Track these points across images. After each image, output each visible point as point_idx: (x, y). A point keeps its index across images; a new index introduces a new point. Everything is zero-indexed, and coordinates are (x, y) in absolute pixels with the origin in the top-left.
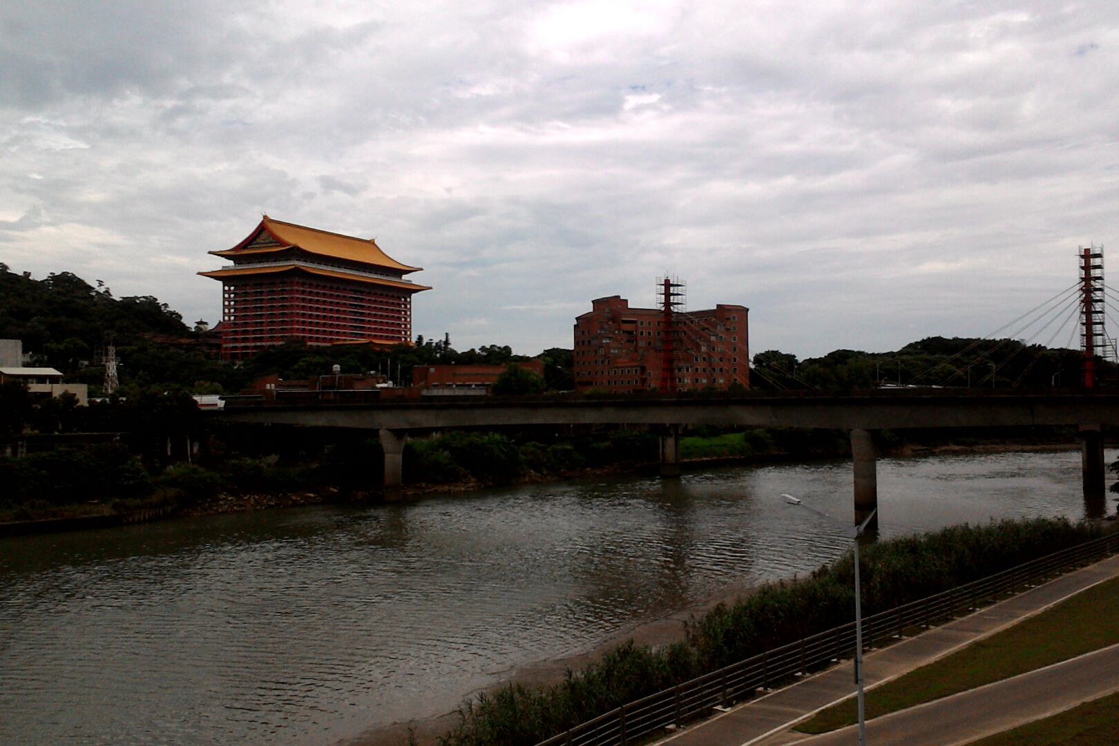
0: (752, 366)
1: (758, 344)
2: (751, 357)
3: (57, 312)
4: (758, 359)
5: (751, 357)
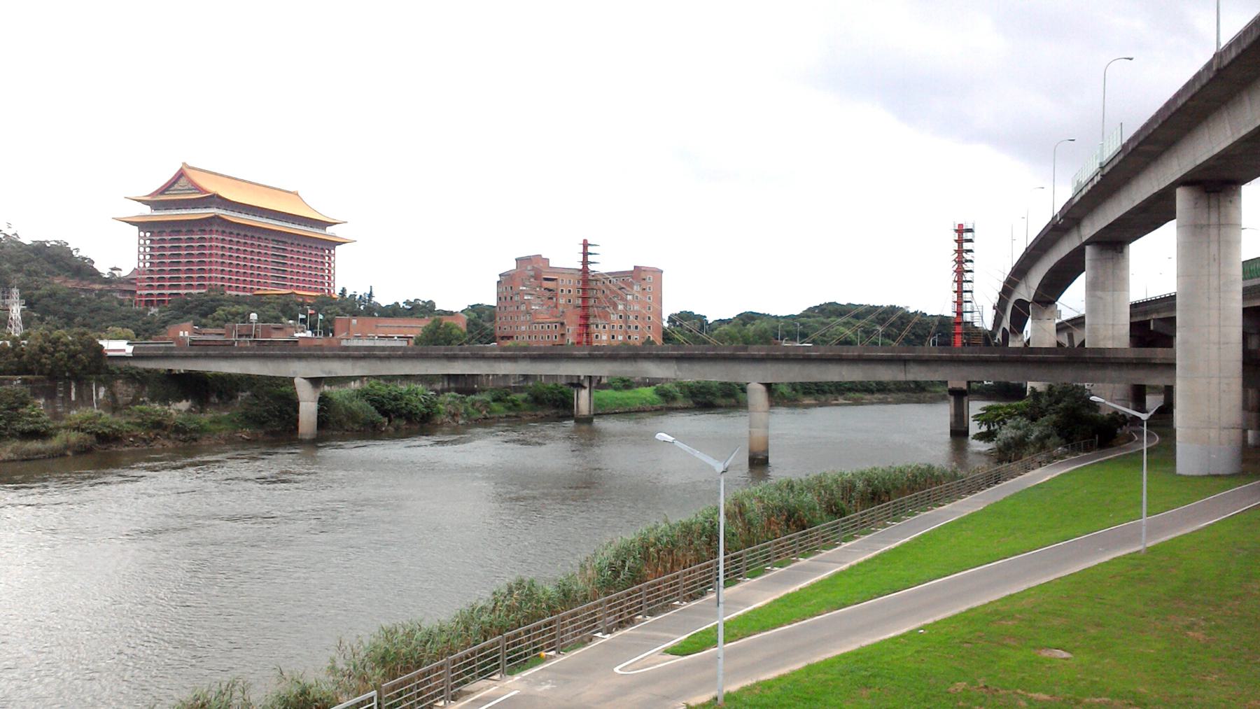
0: (666, 324)
1: (670, 307)
2: (665, 316)
3: (47, 272)
4: (671, 319)
5: (665, 316)
